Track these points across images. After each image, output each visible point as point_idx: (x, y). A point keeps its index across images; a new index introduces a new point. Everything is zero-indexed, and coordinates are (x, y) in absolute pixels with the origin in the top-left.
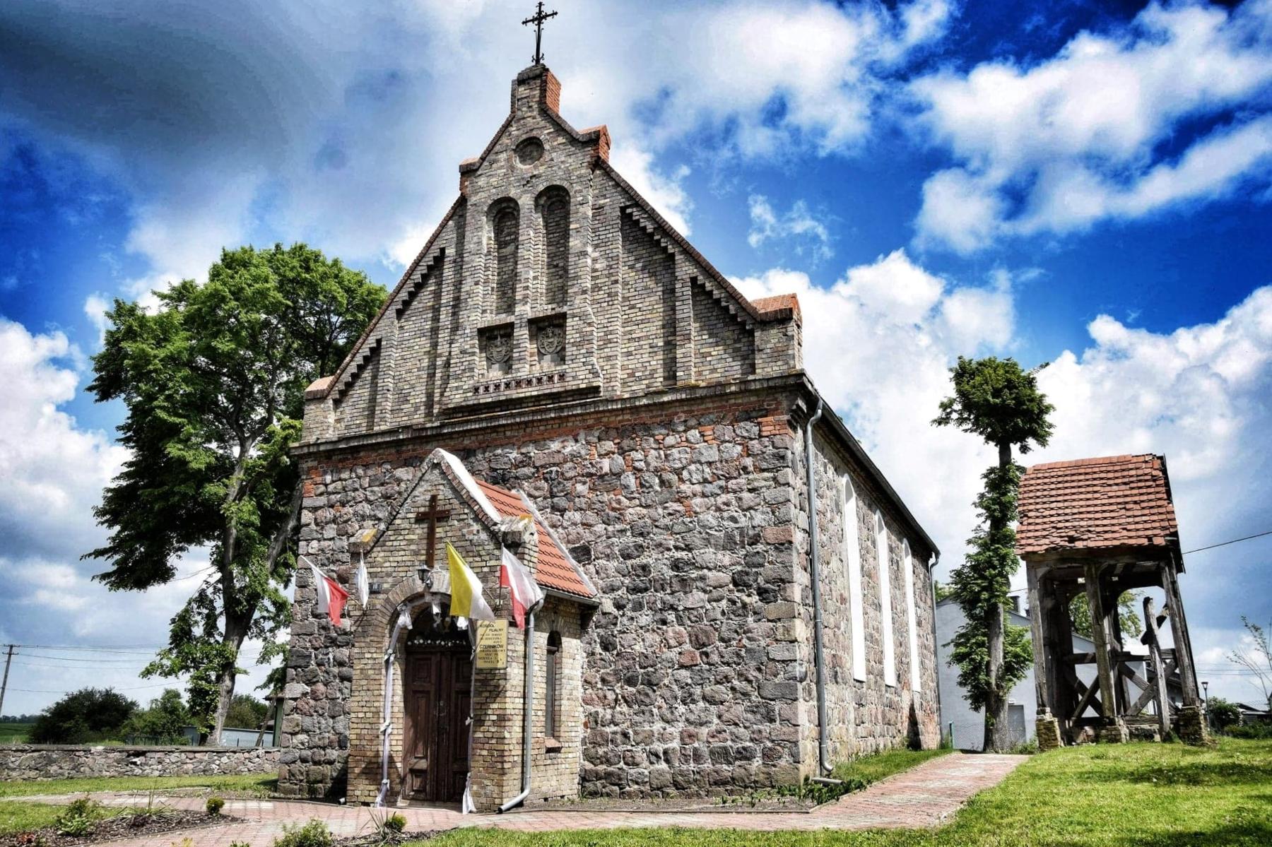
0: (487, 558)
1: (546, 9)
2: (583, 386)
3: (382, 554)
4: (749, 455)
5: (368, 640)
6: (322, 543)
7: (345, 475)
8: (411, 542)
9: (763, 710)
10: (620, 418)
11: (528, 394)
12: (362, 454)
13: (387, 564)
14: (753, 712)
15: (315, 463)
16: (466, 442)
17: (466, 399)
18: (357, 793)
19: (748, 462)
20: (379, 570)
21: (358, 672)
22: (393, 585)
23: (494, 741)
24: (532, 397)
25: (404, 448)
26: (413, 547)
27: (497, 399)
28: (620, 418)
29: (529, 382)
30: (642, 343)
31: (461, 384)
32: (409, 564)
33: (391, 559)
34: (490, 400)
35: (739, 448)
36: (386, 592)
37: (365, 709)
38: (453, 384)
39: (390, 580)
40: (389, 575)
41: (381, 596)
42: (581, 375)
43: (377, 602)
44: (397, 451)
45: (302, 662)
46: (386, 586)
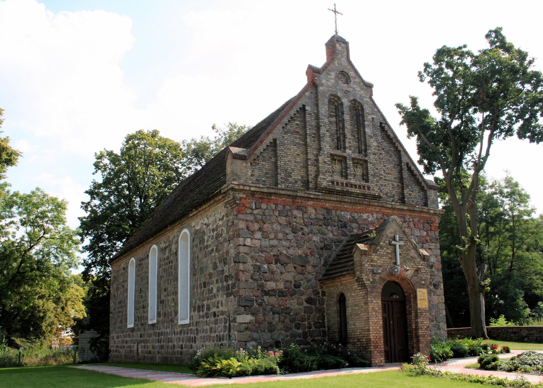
0: (418, 264)
1: (332, 8)
2: (377, 194)
3: (376, 257)
4: (428, 236)
5: (373, 294)
6: (254, 240)
7: (264, 206)
8: (388, 253)
9: (437, 326)
10: (388, 211)
11: (356, 191)
12: (273, 198)
13: (379, 262)
14: (435, 327)
15: (244, 196)
16: (327, 205)
17: (329, 185)
18: (377, 362)
19: (428, 238)
20: (376, 264)
21: (371, 309)
22: (382, 271)
23: (426, 336)
24: (357, 193)
25: (296, 200)
26: (390, 256)
27: (342, 189)
28: (388, 211)
29: (356, 187)
30: (389, 182)
31: (325, 177)
32: (388, 263)
33: (380, 260)
34: (340, 189)
35: (425, 233)
36: (380, 273)
37: (376, 325)
38: (321, 176)
39: (381, 269)
40: (380, 266)
41: (378, 275)
42: (376, 190)
43: (376, 278)
44: (293, 201)
45: (249, 304)
46: (379, 271)
